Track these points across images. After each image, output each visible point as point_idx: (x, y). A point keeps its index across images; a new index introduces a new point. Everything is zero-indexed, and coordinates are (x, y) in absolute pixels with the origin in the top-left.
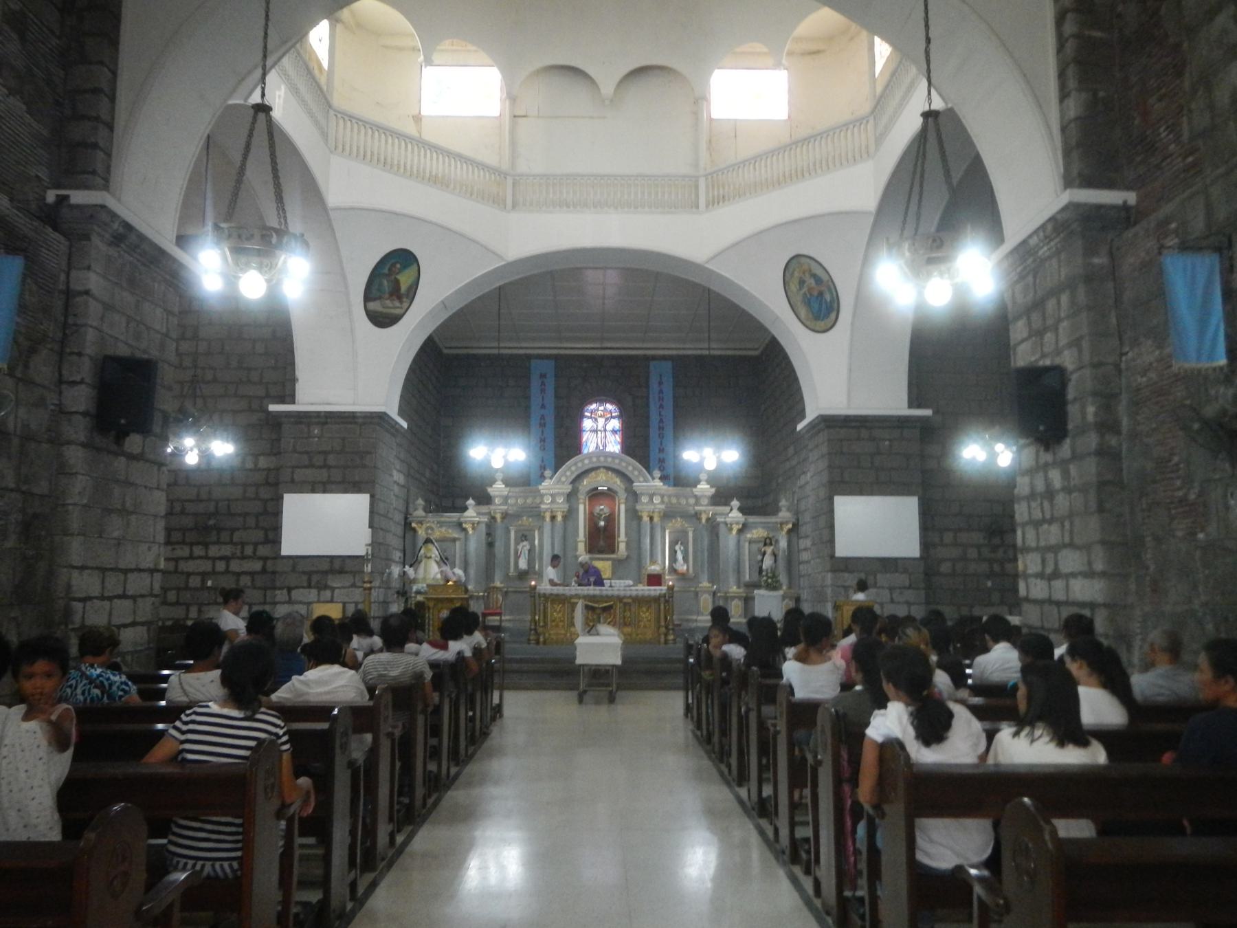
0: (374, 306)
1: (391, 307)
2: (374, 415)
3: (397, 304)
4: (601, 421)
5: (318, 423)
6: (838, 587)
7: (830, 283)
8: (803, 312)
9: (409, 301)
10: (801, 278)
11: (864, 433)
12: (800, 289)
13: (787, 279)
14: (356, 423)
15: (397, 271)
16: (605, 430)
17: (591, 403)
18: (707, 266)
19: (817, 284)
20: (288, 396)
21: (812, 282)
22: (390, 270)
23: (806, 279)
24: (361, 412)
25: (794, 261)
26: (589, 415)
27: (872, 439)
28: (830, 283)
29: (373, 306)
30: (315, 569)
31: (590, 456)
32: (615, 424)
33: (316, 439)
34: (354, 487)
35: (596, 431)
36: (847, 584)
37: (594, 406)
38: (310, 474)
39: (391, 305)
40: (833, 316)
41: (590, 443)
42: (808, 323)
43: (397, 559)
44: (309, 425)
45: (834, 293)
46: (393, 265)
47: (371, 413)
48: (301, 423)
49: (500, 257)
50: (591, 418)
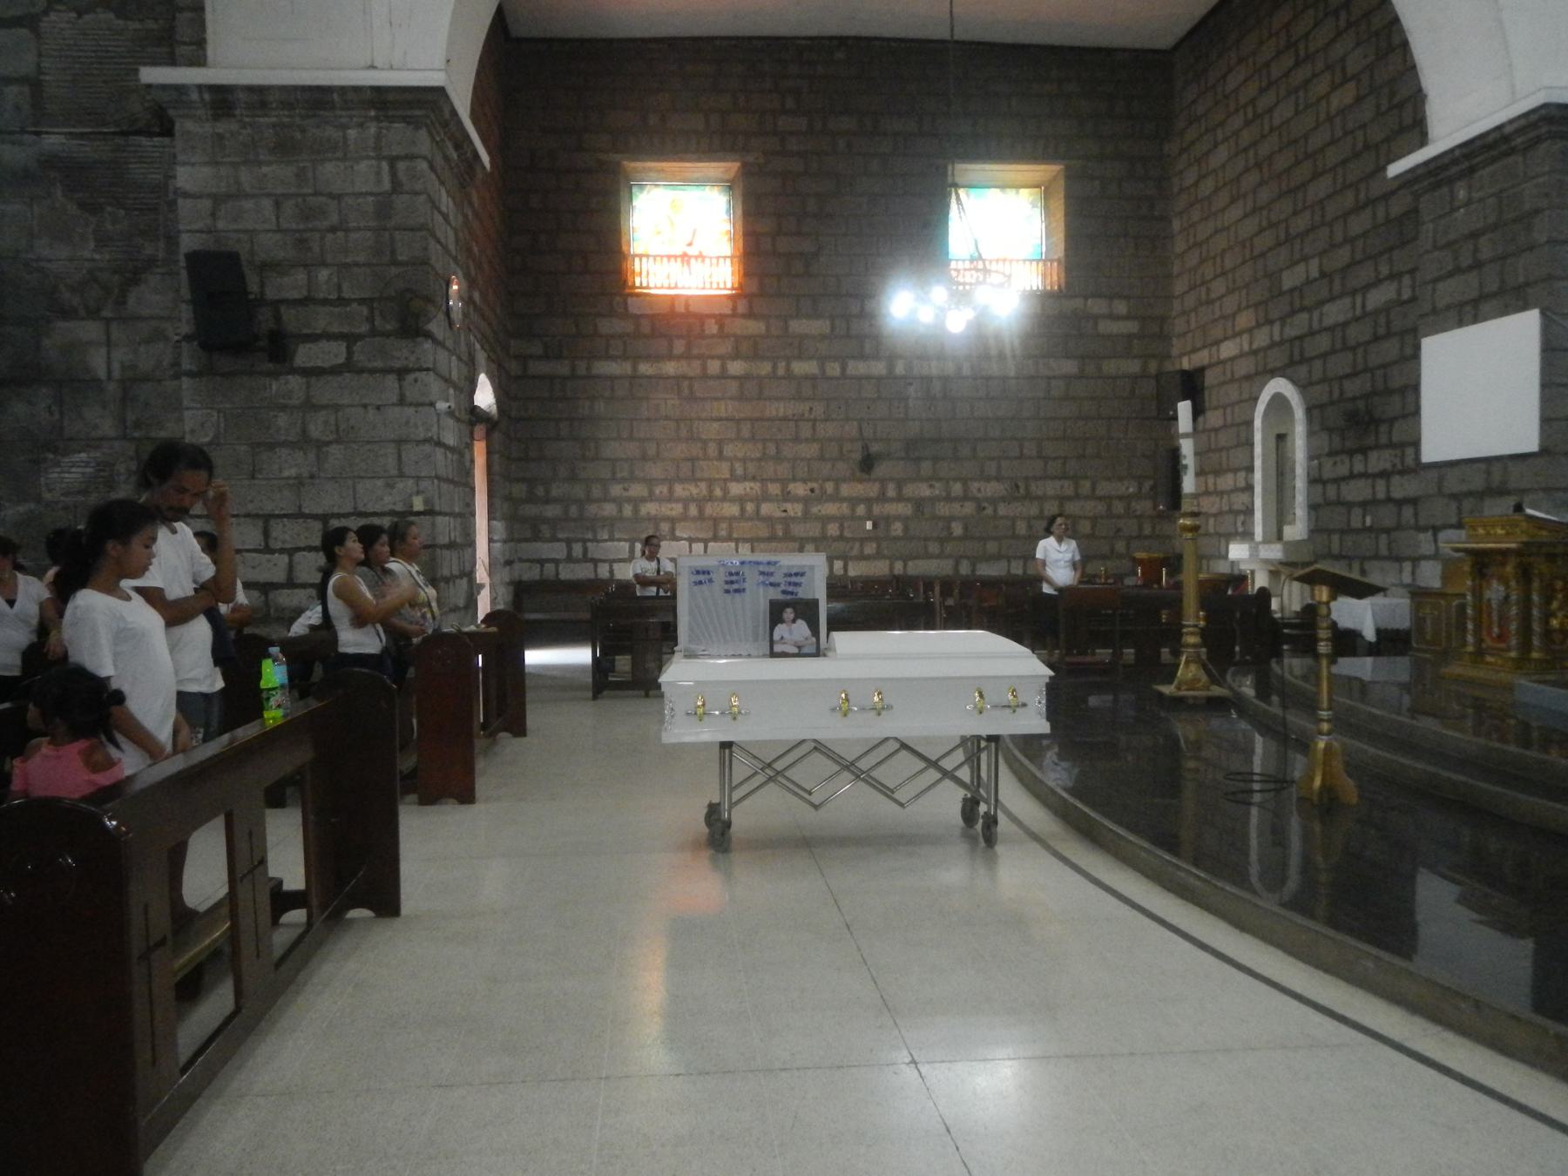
5: (1462, 175)
14: (1513, 151)
20: (1417, 131)
24: (1511, 122)
30: (1465, 488)
33: (1462, 210)
34: (1510, 299)
38: (1450, 291)
44: (1451, 181)
47: (1526, 115)
48: (1437, 186)
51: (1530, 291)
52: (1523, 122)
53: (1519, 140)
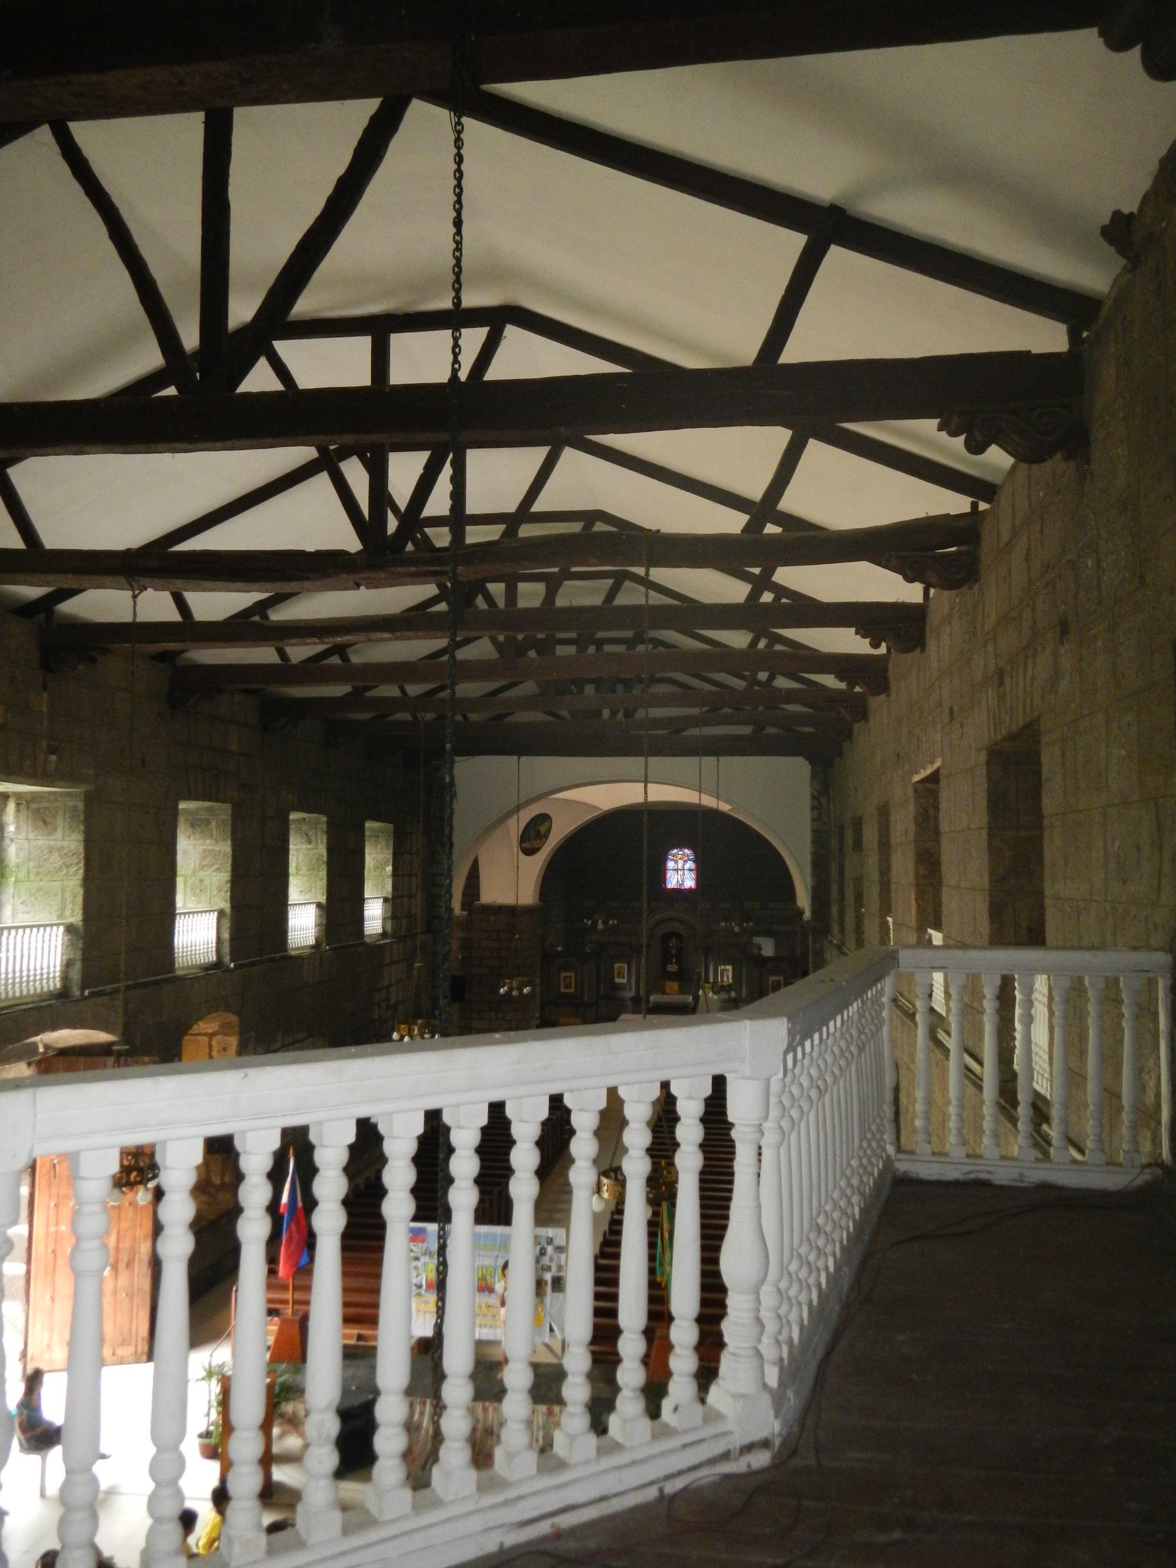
0: (526, 845)
1: (536, 843)
4: (681, 863)
16: (684, 869)
29: (526, 845)
32: (690, 865)
35: (677, 870)
37: (676, 851)
41: (672, 881)
49: (600, 809)
50: (673, 860)
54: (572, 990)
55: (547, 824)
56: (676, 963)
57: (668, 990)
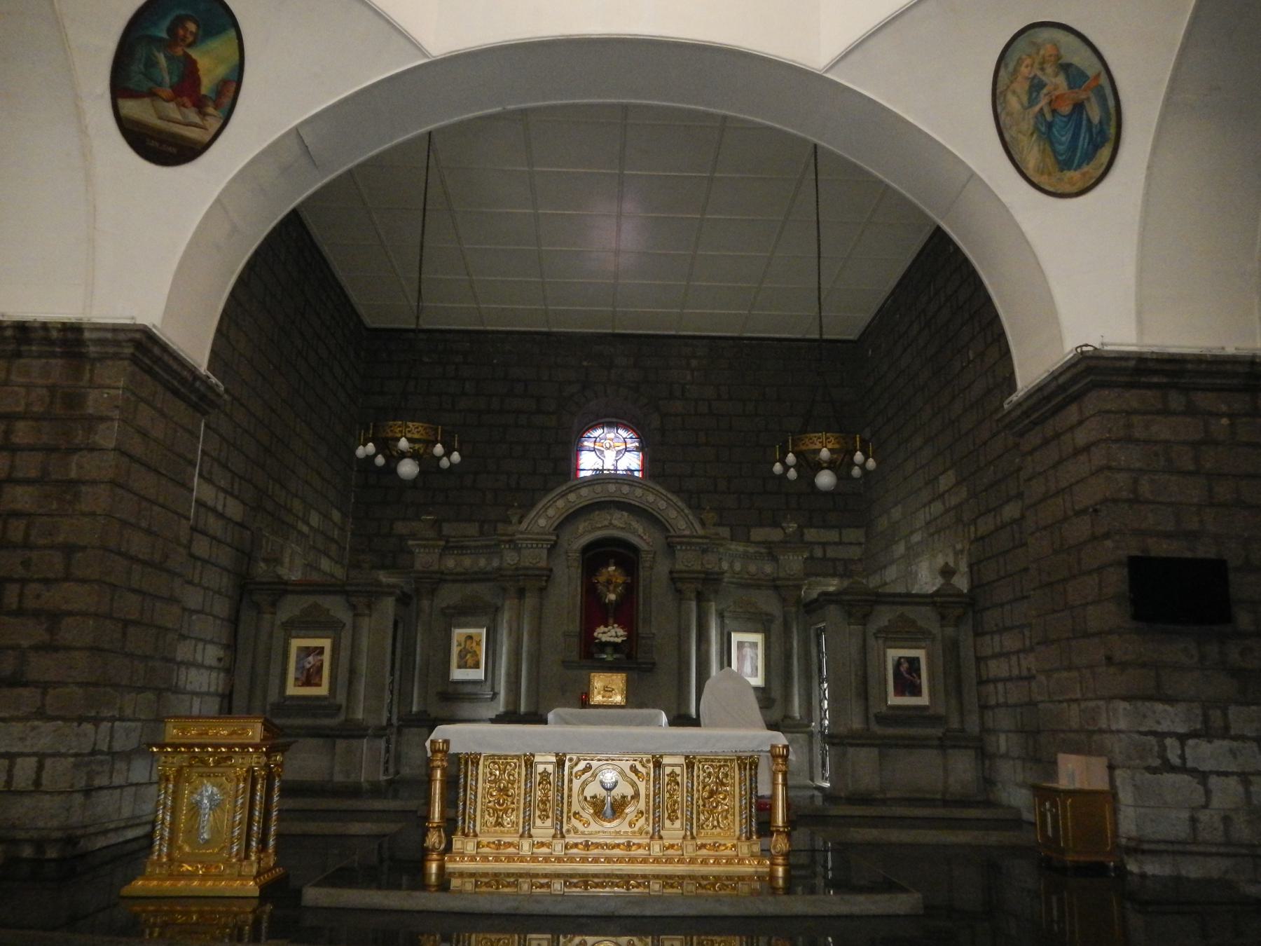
2: (122, 336)
3: (193, 116)
4: (610, 457)
6: (1146, 734)
7: (1104, 80)
8: (1032, 159)
9: (220, 114)
10: (1035, 76)
11: (1176, 401)
12: (1032, 102)
13: (998, 91)
15: (190, 39)
17: (594, 427)
18: (829, 75)
19: (1071, 87)
21: (1061, 81)
22: (172, 31)
23: (1044, 78)
25: (1022, 43)
26: (592, 445)
27: (1190, 410)
28: (1104, 80)
29: (133, 108)
31: (589, 482)
36: (1164, 727)
39: (179, 117)
40: (1105, 153)
42: (1043, 180)
43: (214, 663)
45: (1111, 103)
46: (179, 21)
51: (84, 489)
52: (109, 335)
53: (92, 349)
54: (323, 690)
55: (221, 46)
56: (622, 624)
57: (597, 698)
